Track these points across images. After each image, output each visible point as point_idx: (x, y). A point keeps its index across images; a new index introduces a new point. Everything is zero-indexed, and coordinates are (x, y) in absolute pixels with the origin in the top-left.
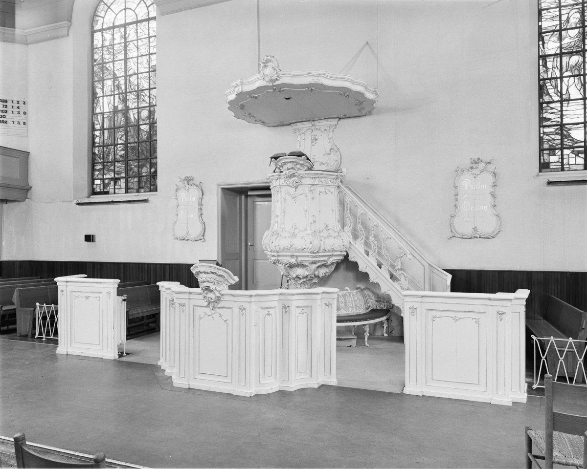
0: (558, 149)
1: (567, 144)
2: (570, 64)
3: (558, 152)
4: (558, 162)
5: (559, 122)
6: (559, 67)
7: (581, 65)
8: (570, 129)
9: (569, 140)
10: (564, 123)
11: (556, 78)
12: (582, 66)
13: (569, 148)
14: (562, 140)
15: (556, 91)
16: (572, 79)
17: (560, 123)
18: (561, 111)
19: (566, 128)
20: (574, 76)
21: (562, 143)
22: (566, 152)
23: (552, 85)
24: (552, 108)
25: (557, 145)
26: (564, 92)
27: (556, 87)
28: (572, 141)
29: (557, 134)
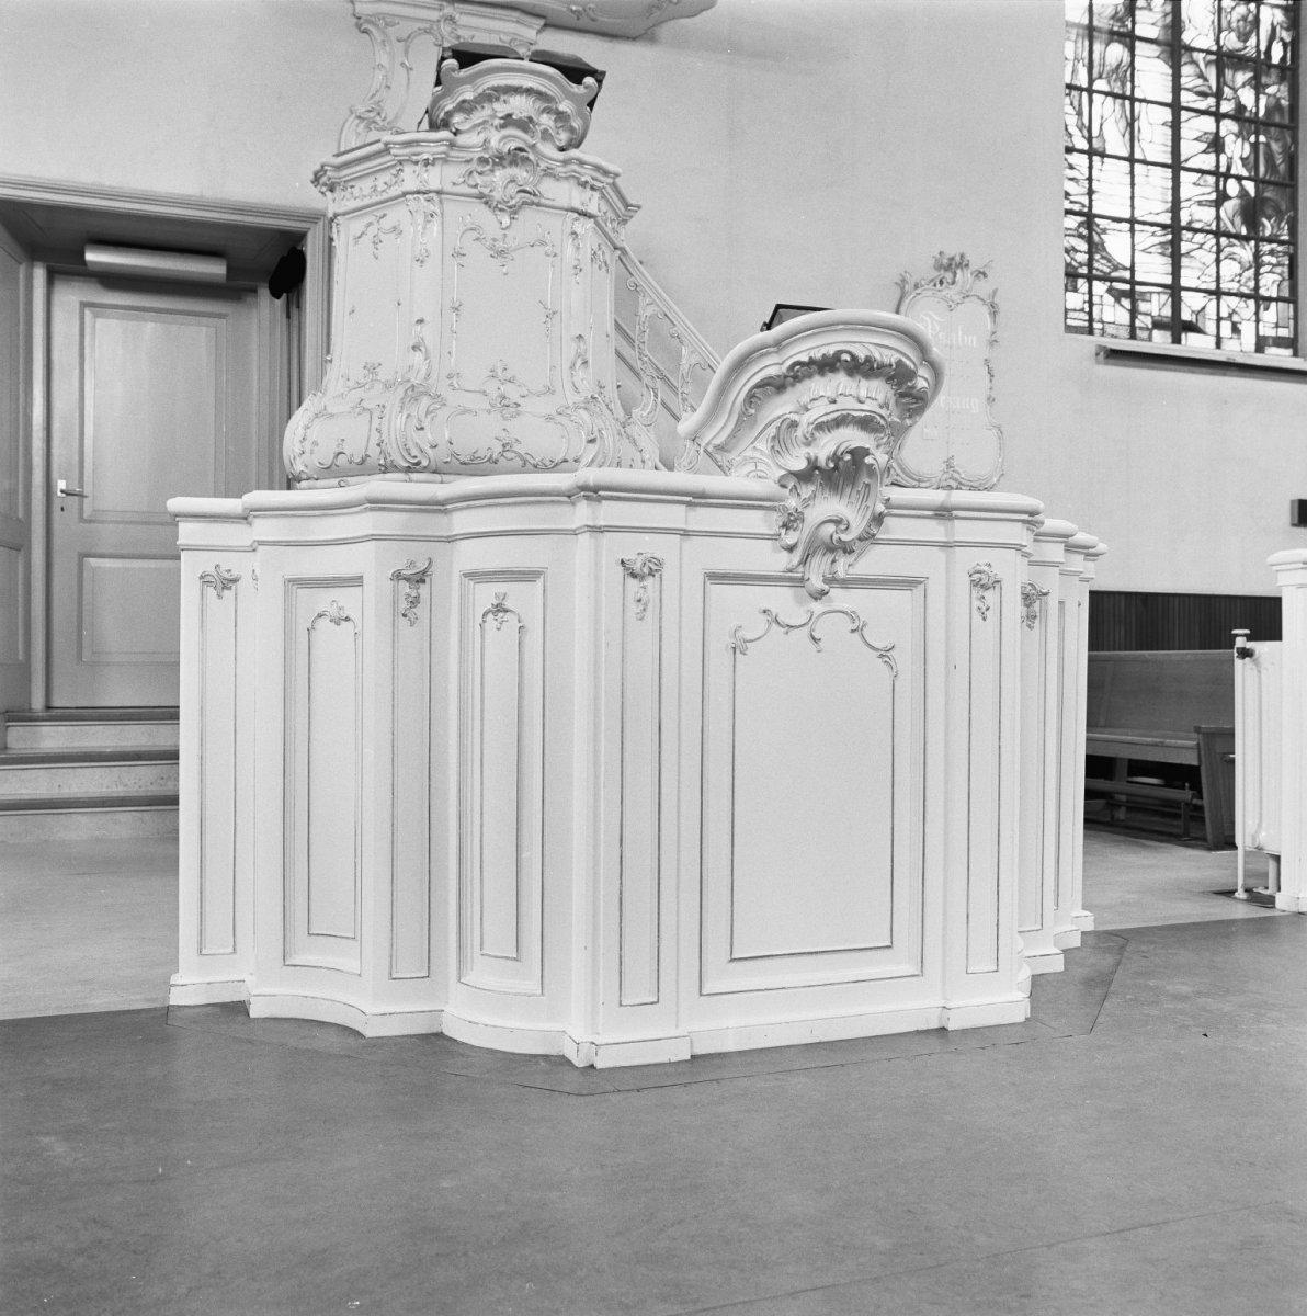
0: (1082, 276)
1: (1100, 267)
2: (1108, 61)
3: (1082, 284)
4: (1082, 310)
5: (1084, 206)
6: (1086, 61)
7: (1126, 72)
8: (1104, 231)
9: (1103, 257)
10: (1095, 211)
11: (1080, 89)
12: (1129, 73)
13: (1105, 278)
14: (1090, 253)
15: (1080, 123)
16: (1110, 99)
17: (1086, 210)
18: (1090, 179)
19: (1098, 226)
20: (1115, 96)
21: (1090, 264)
22: (1100, 288)
23: (1072, 104)
24: (1071, 167)
25: (1081, 265)
26: (1095, 132)
27: (1079, 113)
28: (1109, 261)
29: (1080, 236)
